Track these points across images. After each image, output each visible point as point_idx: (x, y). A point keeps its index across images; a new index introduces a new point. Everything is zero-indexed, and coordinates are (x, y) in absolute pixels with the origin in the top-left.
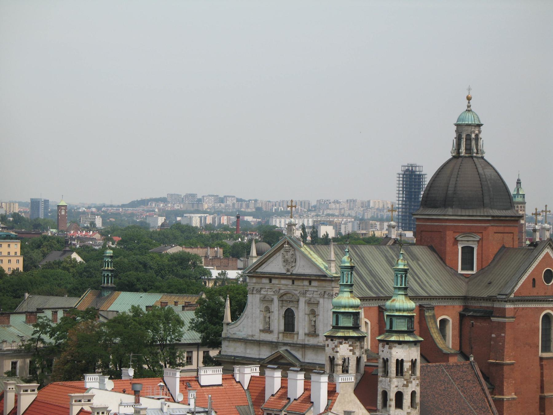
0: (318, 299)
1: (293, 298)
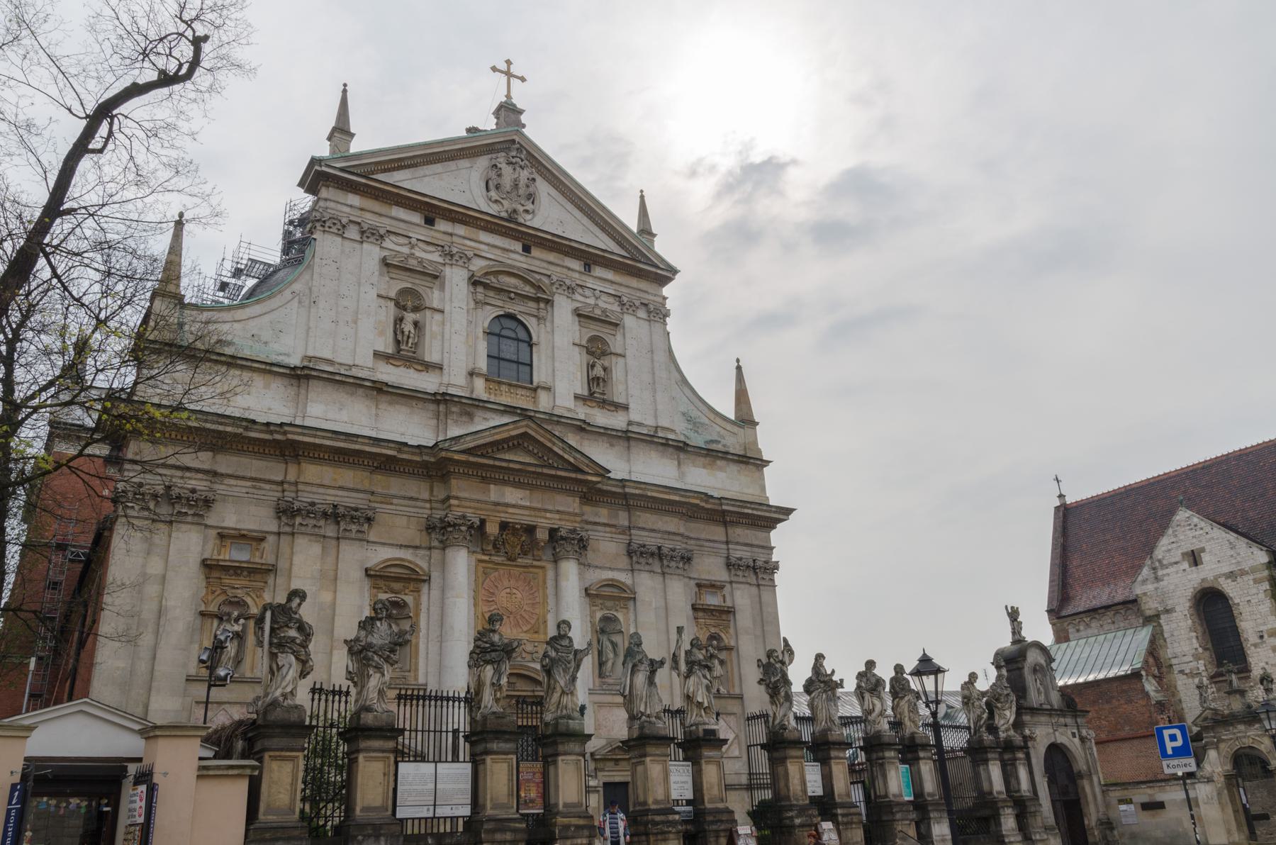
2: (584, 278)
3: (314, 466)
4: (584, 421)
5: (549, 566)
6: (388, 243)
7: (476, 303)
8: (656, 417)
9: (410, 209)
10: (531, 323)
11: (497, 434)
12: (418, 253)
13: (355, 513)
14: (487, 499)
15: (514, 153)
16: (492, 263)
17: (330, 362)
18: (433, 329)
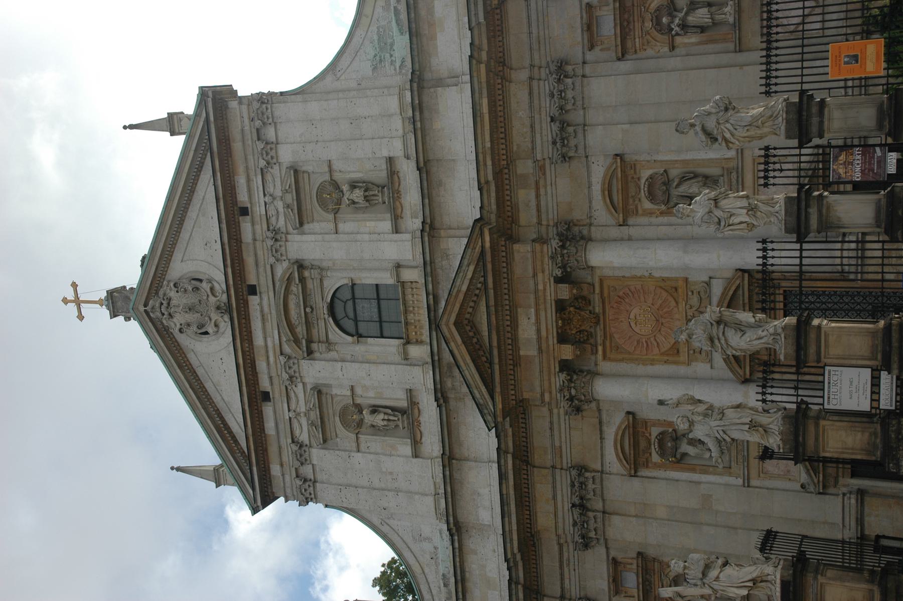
0: (283, 173)
1: (296, 293)
2: (257, 219)
3: (538, 519)
4: (422, 231)
5: (598, 273)
6: (304, 437)
7: (330, 350)
8: (391, 116)
9: (262, 418)
10: (332, 284)
11: (464, 360)
12: (303, 409)
13: (577, 485)
14: (537, 360)
15: (159, 315)
16: (282, 335)
17: (436, 503)
18: (373, 395)
